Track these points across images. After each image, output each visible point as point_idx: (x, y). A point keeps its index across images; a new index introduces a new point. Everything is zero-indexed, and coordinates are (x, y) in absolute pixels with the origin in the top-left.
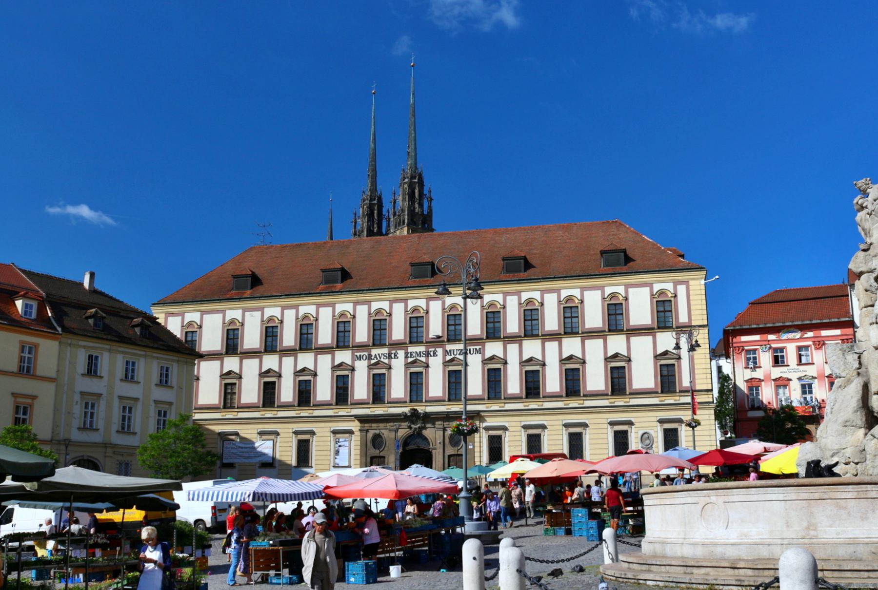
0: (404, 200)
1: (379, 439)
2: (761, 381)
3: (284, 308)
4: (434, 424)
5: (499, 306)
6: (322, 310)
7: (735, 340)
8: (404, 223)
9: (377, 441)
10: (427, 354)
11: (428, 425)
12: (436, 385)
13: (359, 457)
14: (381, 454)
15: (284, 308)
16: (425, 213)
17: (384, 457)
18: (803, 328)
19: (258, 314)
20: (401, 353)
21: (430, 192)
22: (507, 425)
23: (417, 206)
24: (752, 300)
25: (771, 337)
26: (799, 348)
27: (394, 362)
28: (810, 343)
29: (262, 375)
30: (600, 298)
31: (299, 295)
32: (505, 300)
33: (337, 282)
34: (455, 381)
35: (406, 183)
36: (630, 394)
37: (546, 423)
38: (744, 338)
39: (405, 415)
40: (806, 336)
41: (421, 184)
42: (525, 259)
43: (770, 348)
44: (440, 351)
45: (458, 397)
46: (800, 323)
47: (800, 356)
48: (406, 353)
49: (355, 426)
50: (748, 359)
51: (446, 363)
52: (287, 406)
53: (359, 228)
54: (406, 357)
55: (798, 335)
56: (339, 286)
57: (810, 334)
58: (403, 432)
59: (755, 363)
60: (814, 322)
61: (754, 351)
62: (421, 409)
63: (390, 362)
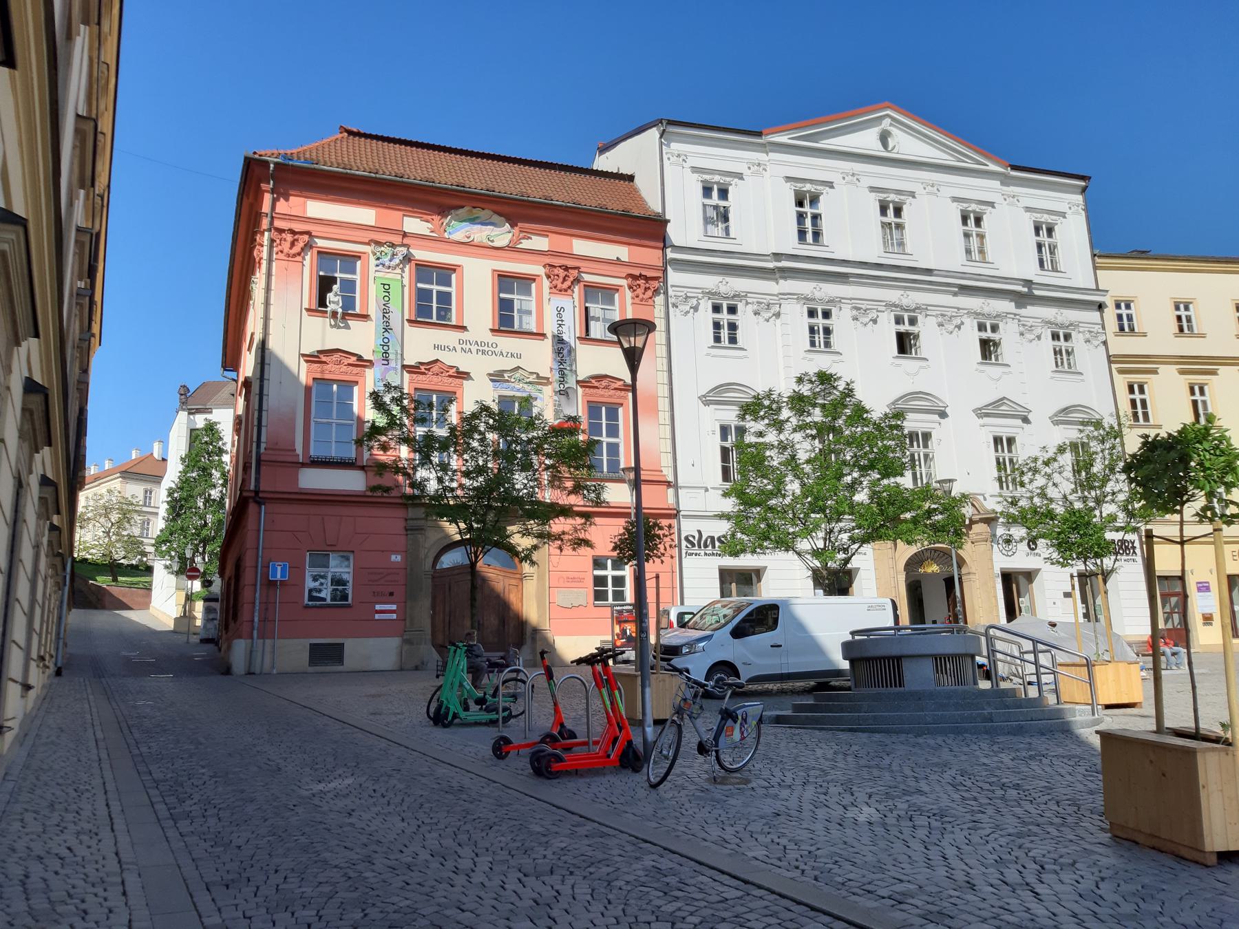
7: (282, 206)
25: (414, 224)
26: (505, 281)
38: (317, 208)
43: (408, 259)
50: (325, 285)
55: (502, 235)
57: (539, 243)
59: (349, 303)
61: (350, 260)
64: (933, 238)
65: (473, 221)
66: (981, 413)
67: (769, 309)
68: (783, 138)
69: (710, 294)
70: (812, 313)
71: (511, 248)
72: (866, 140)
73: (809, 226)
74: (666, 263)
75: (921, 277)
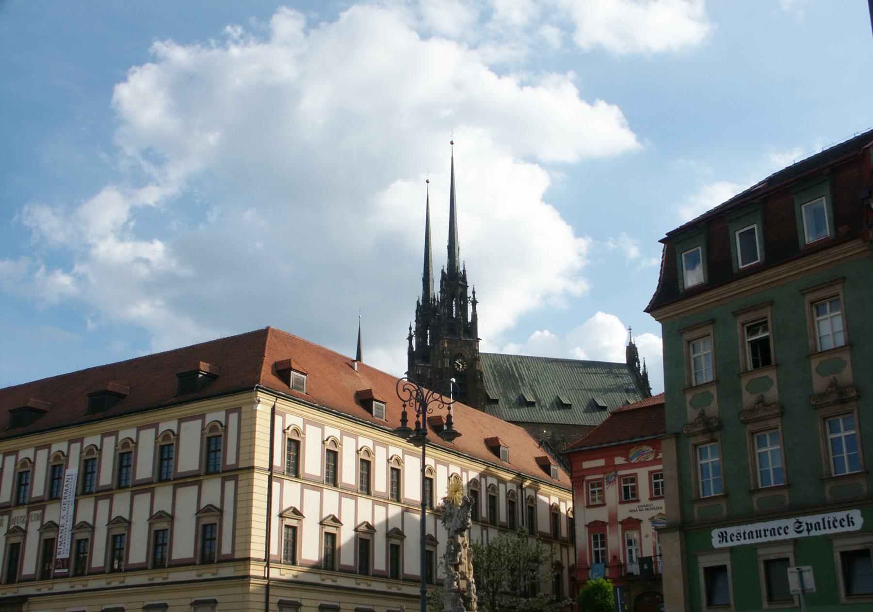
2: (604, 524)
16: (469, 320)
21: (474, 293)
25: (619, 460)
30: (153, 438)
36: (219, 562)
38: (587, 465)
71: (656, 461)
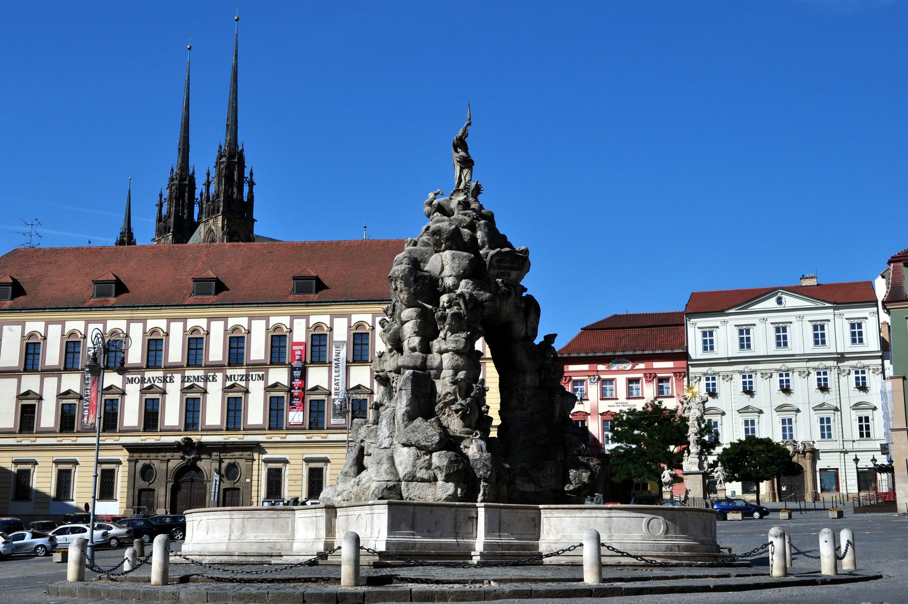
0: (219, 183)
1: (150, 470)
2: (587, 414)
3: (48, 323)
4: (210, 455)
5: (285, 330)
6: (91, 327)
8: (218, 212)
9: (147, 472)
10: (206, 379)
11: (203, 456)
12: (213, 414)
13: (126, 489)
14: (151, 487)
15: (48, 323)
16: (245, 199)
17: (154, 490)
18: (635, 359)
19: (18, 328)
20: (177, 377)
21: (251, 174)
22: (287, 457)
23: (235, 190)
24: (585, 325)
25: (601, 367)
26: (630, 381)
27: (169, 386)
28: (641, 375)
29: (20, 397)
31: (66, 309)
32: (292, 323)
33: (110, 296)
34: (234, 409)
35: (223, 163)
37: (329, 457)
38: (572, 368)
39: (178, 444)
40: (637, 367)
41: (241, 164)
42: (317, 279)
43: (599, 379)
44: (220, 376)
45: (237, 426)
46: (631, 353)
47: (629, 391)
48: (183, 378)
49: (123, 455)
51: (226, 390)
52: (47, 432)
53: (164, 212)
54: (183, 381)
55: (629, 366)
56: (112, 300)
57: (641, 366)
58: (173, 464)
60: (646, 352)
61: (582, 382)
62: (195, 439)
63: (165, 386)
64: (800, 339)
65: (619, 363)
66: (815, 409)
67: (728, 378)
68: (733, 311)
69: (705, 374)
70: (744, 377)
71: (632, 370)
72: (771, 303)
73: (745, 343)
74: (688, 365)
75: (792, 358)
